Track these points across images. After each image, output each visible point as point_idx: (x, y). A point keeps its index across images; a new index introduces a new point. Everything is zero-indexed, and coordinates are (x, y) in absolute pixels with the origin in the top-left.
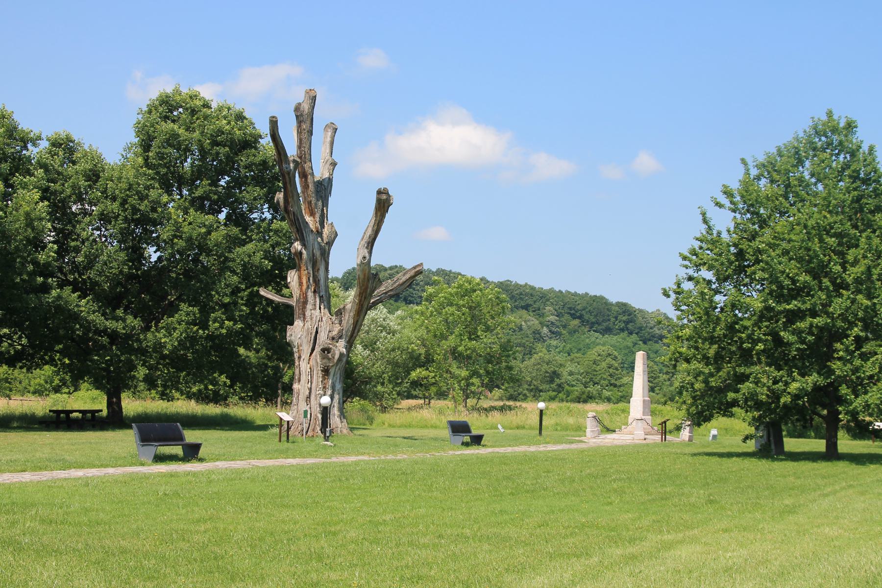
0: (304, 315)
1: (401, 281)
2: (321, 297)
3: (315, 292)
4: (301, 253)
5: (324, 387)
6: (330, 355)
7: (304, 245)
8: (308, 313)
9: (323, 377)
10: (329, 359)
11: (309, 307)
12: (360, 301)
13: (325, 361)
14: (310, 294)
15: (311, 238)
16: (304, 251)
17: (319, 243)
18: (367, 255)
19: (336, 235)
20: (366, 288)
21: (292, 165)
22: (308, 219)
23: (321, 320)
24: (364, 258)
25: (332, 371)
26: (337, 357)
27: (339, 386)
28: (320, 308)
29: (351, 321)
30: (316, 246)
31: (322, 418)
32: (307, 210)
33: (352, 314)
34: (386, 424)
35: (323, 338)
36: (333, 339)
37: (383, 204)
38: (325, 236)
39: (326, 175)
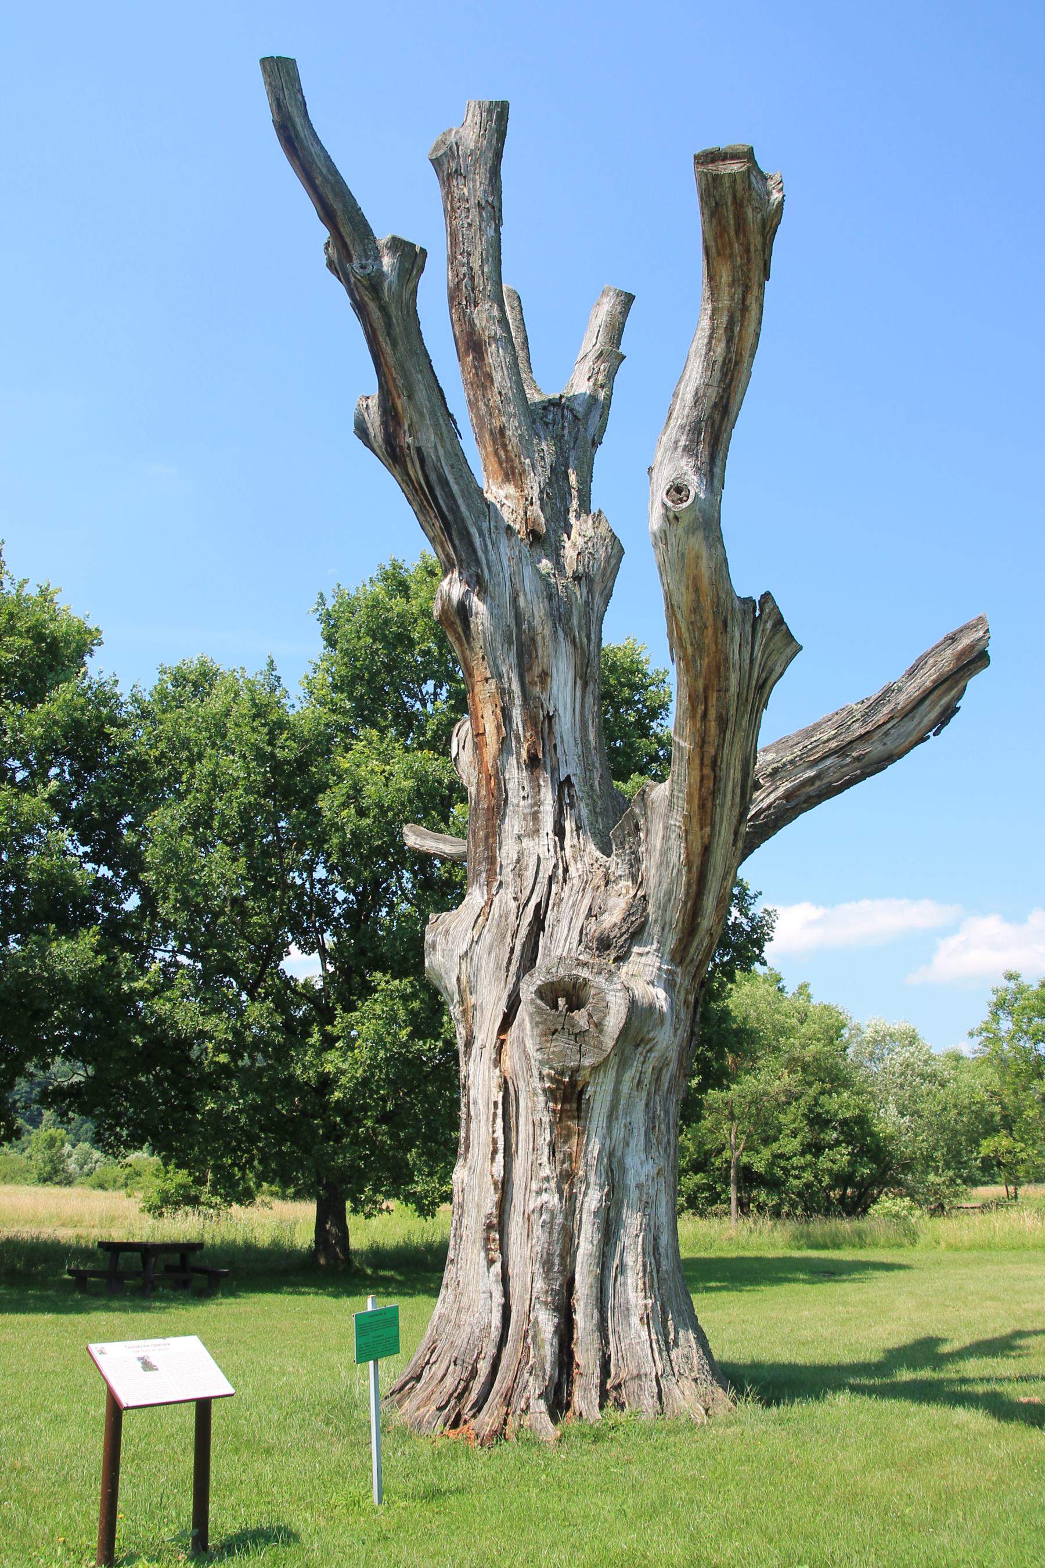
0: (492, 860)
1: (902, 700)
2: (563, 786)
3: (533, 763)
4: (463, 611)
5: (567, 1177)
6: (580, 1017)
7: (478, 583)
8: (507, 852)
9: (559, 1119)
10: (579, 1036)
11: (513, 825)
12: (702, 743)
13: (560, 1044)
14: (515, 776)
15: (503, 556)
16: (478, 606)
17: (544, 578)
18: (695, 485)
19: (622, 551)
20: (719, 668)
21: (387, 262)
22: (498, 493)
23: (561, 874)
24: (678, 490)
25: (599, 1094)
26: (615, 1021)
27: (640, 1167)
28: (559, 832)
29: (677, 853)
30: (529, 582)
31: (558, 1331)
32: (493, 465)
33: (677, 820)
34: (943, 1244)
35: (561, 944)
36: (604, 944)
37: (739, 219)
38: (569, 553)
39: (581, 386)
